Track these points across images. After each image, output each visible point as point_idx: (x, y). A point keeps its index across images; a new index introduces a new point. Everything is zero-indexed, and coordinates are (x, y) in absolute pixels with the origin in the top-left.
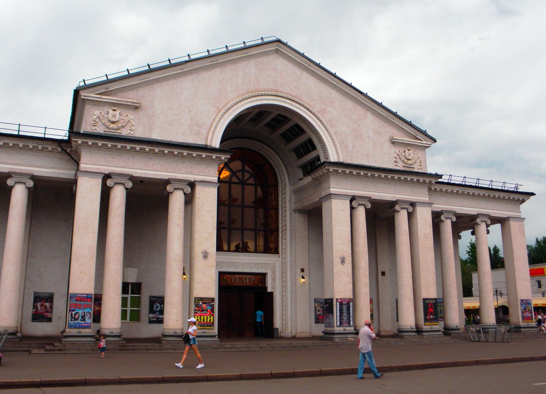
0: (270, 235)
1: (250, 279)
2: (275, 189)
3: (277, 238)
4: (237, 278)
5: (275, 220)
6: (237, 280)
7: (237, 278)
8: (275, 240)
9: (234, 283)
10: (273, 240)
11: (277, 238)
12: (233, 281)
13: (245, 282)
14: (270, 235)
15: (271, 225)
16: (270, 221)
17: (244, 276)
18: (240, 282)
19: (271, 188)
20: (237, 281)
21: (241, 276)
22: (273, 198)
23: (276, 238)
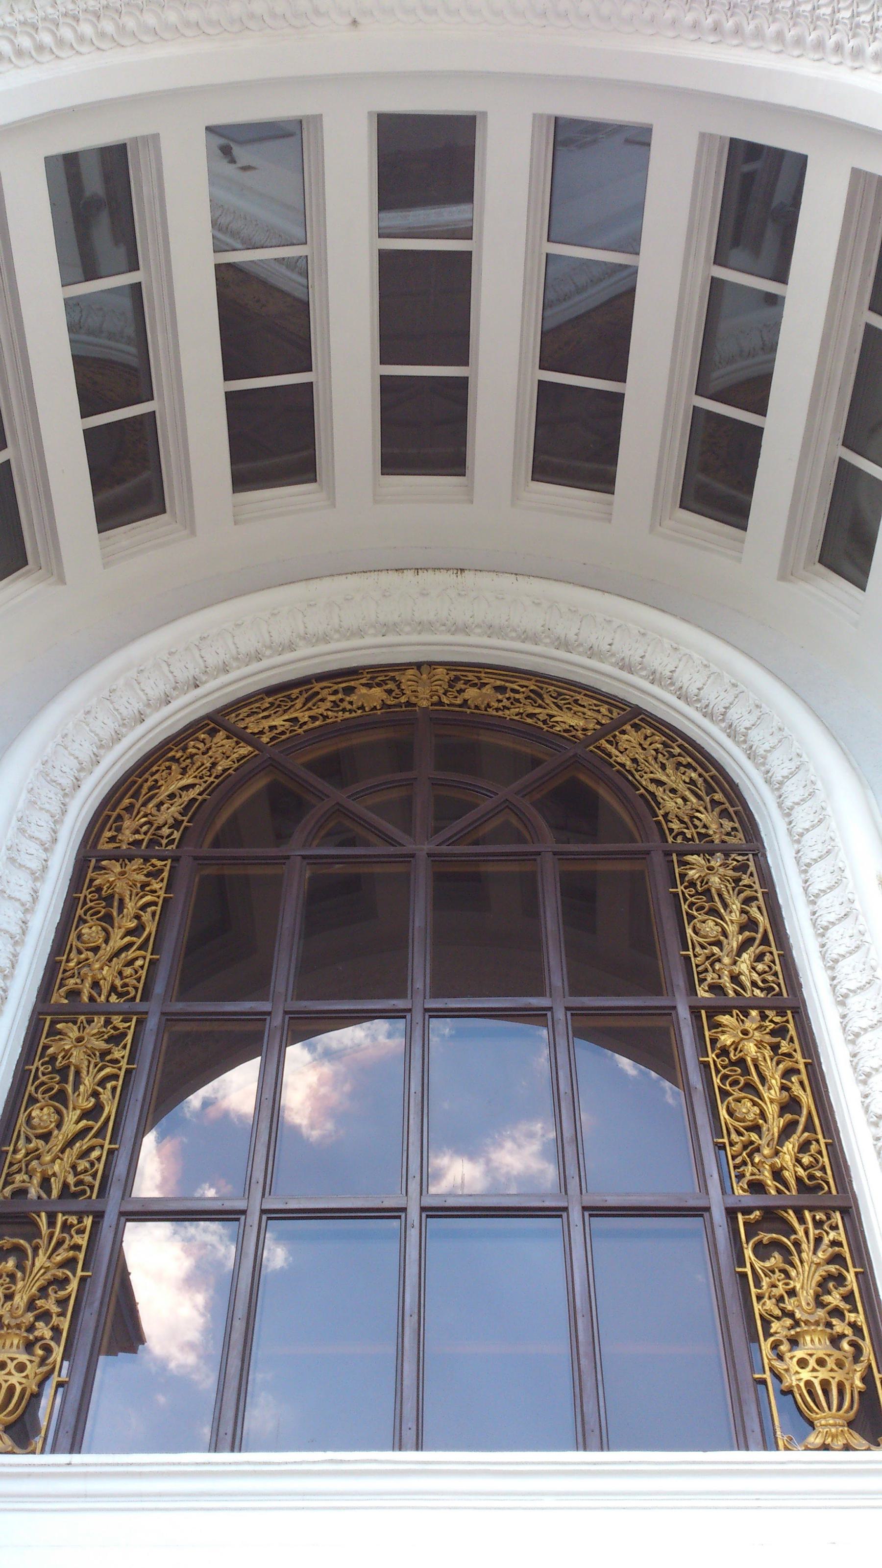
0: (762, 1252)
2: (743, 868)
3: (851, 1277)
5: (791, 1105)
8: (834, 1299)
10: (806, 1296)
14: (762, 1252)
15: (752, 1149)
16: (731, 1113)
23: (840, 1280)
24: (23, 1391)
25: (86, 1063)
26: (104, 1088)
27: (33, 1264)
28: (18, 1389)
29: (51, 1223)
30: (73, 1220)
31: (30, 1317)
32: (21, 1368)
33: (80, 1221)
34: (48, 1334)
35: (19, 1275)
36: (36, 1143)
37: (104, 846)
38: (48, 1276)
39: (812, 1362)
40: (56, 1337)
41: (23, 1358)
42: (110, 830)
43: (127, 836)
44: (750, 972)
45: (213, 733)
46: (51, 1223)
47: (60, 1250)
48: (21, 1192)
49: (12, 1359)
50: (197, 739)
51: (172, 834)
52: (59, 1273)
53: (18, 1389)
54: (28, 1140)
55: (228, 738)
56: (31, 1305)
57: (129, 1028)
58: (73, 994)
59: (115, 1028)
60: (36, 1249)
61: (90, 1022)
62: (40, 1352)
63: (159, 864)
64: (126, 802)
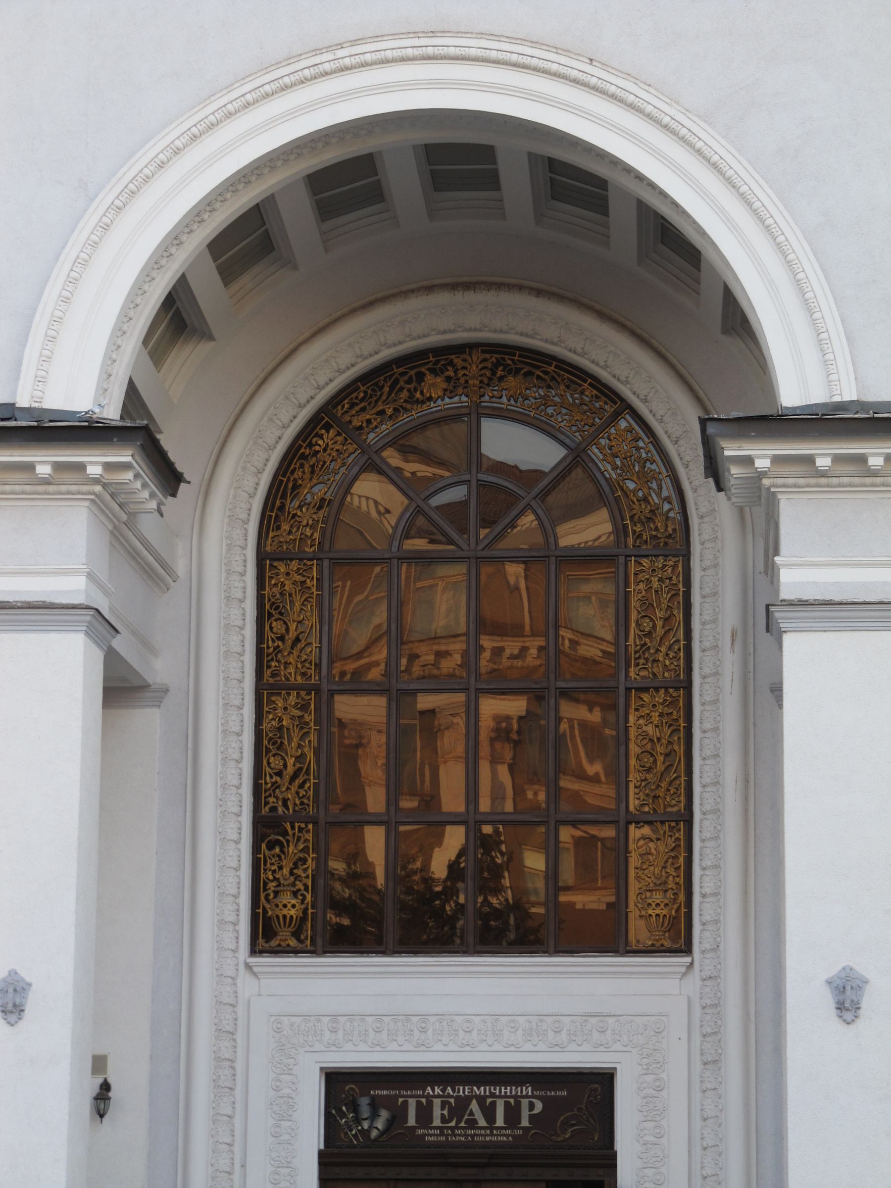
1: (512, 1114)
4: (437, 1102)
6: (437, 1112)
7: (437, 1102)
9: (420, 1132)
11: (681, 860)
12: (412, 1121)
13: (482, 1122)
17: (480, 1091)
18: (453, 1124)
19: (646, 562)
20: (437, 1122)
21: (464, 1091)
22: (659, 623)
24: (297, 917)
25: (291, 725)
26: (305, 742)
27: (288, 851)
28: (295, 917)
29: (293, 828)
30: (303, 825)
31: (292, 879)
32: (294, 906)
33: (307, 826)
34: (302, 888)
35: (283, 857)
36: (275, 778)
38: (297, 857)
39: (654, 905)
40: (306, 889)
41: (294, 901)
42: (273, 531)
44: (665, 659)
46: (293, 828)
47: (300, 844)
48: (274, 809)
49: (289, 903)
50: (317, 435)
51: (312, 535)
52: (301, 855)
53: (295, 917)
54: (271, 777)
55: (339, 434)
56: (291, 873)
57: (311, 699)
59: (303, 699)
60: (288, 841)
61: (289, 694)
62: (301, 898)
63: (309, 563)
64: (278, 503)
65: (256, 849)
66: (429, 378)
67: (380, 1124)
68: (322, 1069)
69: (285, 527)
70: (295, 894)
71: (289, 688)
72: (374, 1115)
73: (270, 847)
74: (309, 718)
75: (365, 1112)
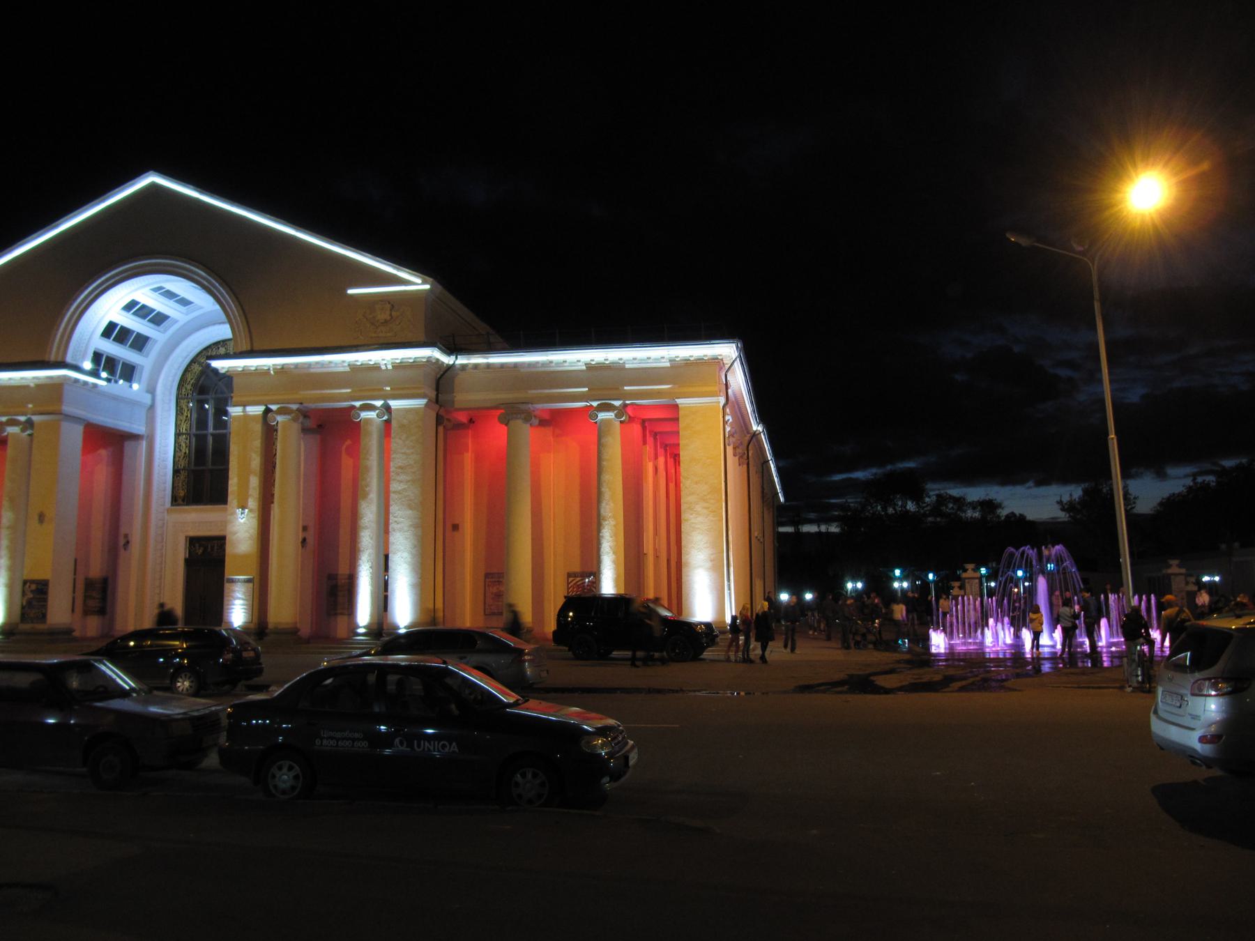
4: (216, 545)
6: (216, 548)
7: (216, 545)
12: (209, 550)
37: (180, 396)
43: (183, 393)
45: (195, 363)
58: (180, 430)
65: (173, 478)
66: (220, 349)
67: (201, 551)
68: (186, 537)
69: (184, 390)
70: (183, 490)
71: (183, 434)
72: (199, 549)
73: (177, 477)
74: (188, 442)
75: (197, 547)
